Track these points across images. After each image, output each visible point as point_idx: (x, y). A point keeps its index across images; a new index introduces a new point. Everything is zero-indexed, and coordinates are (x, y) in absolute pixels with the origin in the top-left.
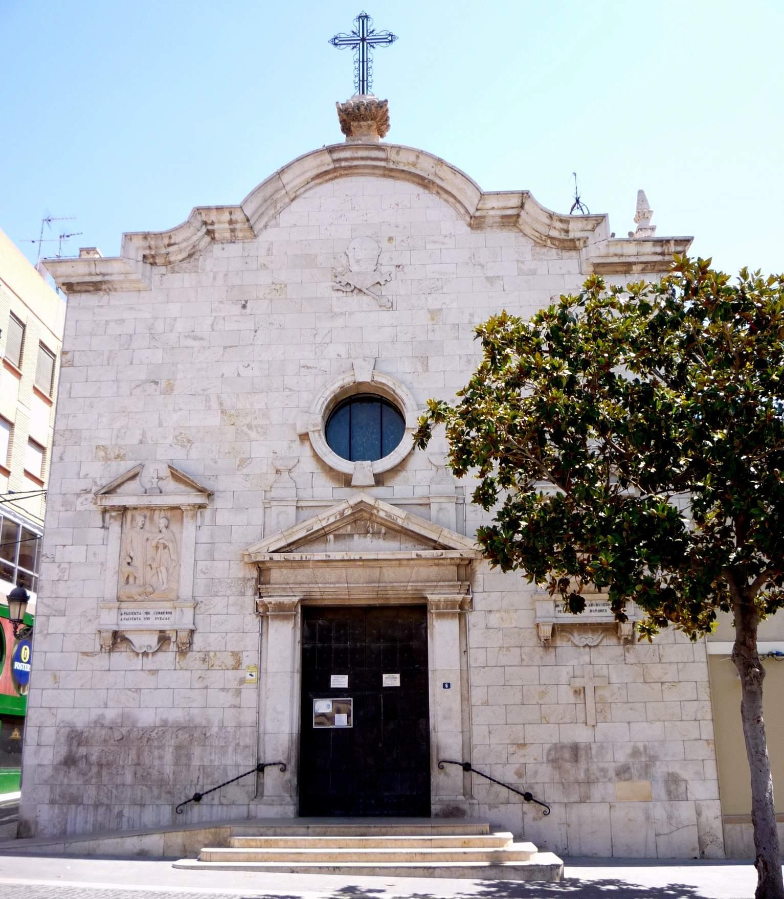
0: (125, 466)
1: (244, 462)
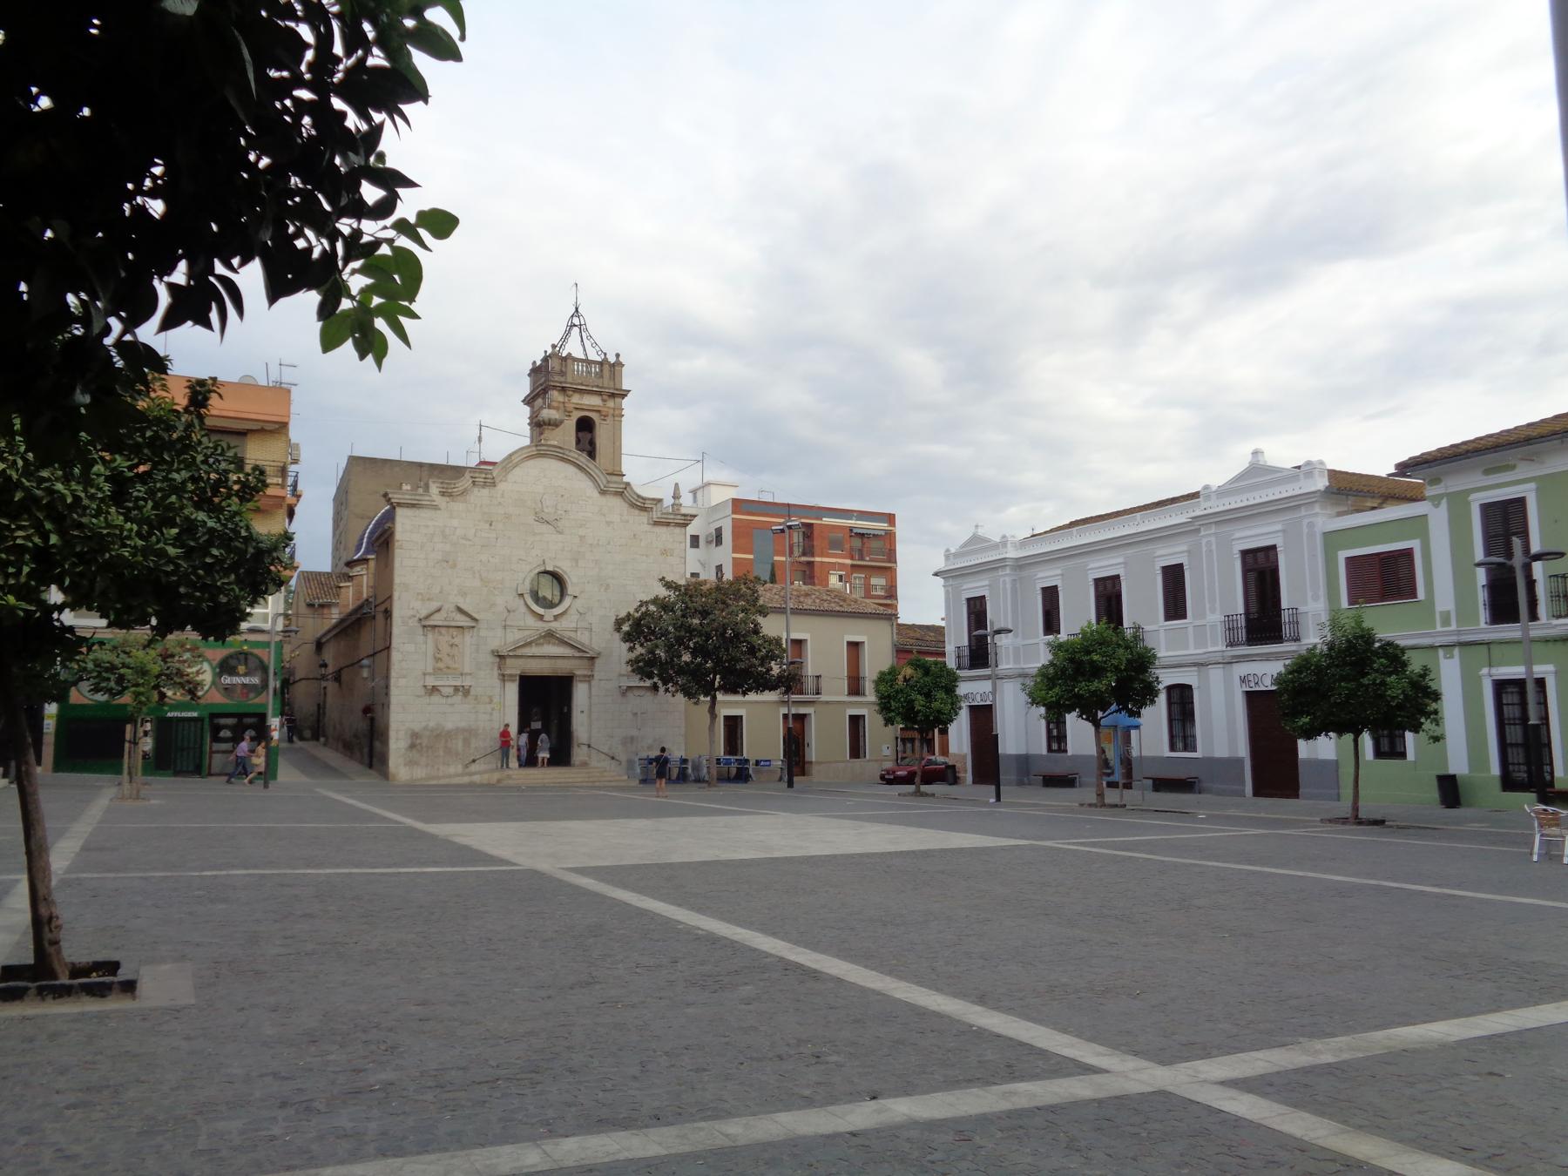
0: (435, 605)
1: (493, 605)
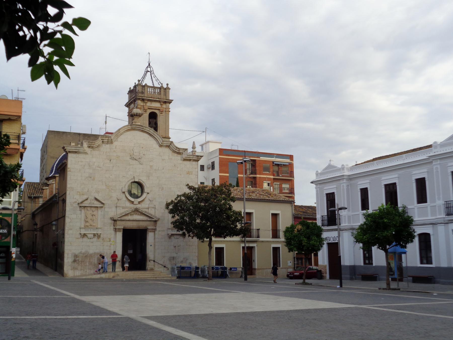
0: (85, 197)
